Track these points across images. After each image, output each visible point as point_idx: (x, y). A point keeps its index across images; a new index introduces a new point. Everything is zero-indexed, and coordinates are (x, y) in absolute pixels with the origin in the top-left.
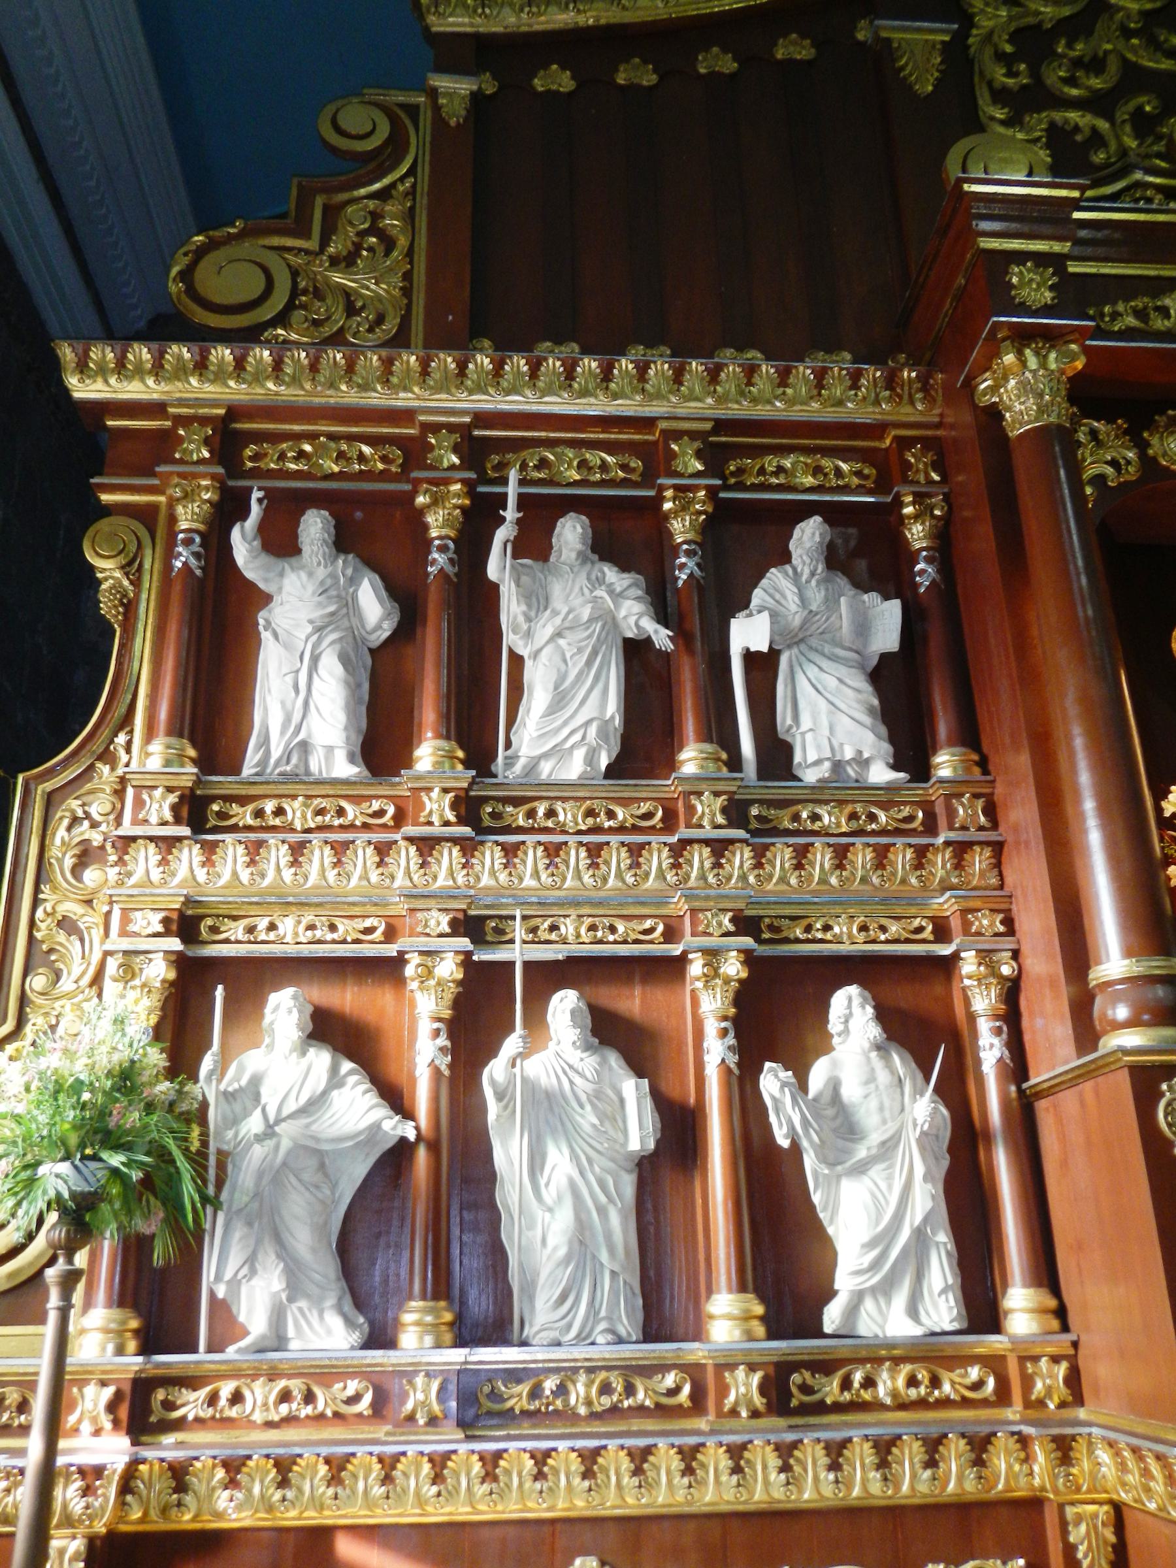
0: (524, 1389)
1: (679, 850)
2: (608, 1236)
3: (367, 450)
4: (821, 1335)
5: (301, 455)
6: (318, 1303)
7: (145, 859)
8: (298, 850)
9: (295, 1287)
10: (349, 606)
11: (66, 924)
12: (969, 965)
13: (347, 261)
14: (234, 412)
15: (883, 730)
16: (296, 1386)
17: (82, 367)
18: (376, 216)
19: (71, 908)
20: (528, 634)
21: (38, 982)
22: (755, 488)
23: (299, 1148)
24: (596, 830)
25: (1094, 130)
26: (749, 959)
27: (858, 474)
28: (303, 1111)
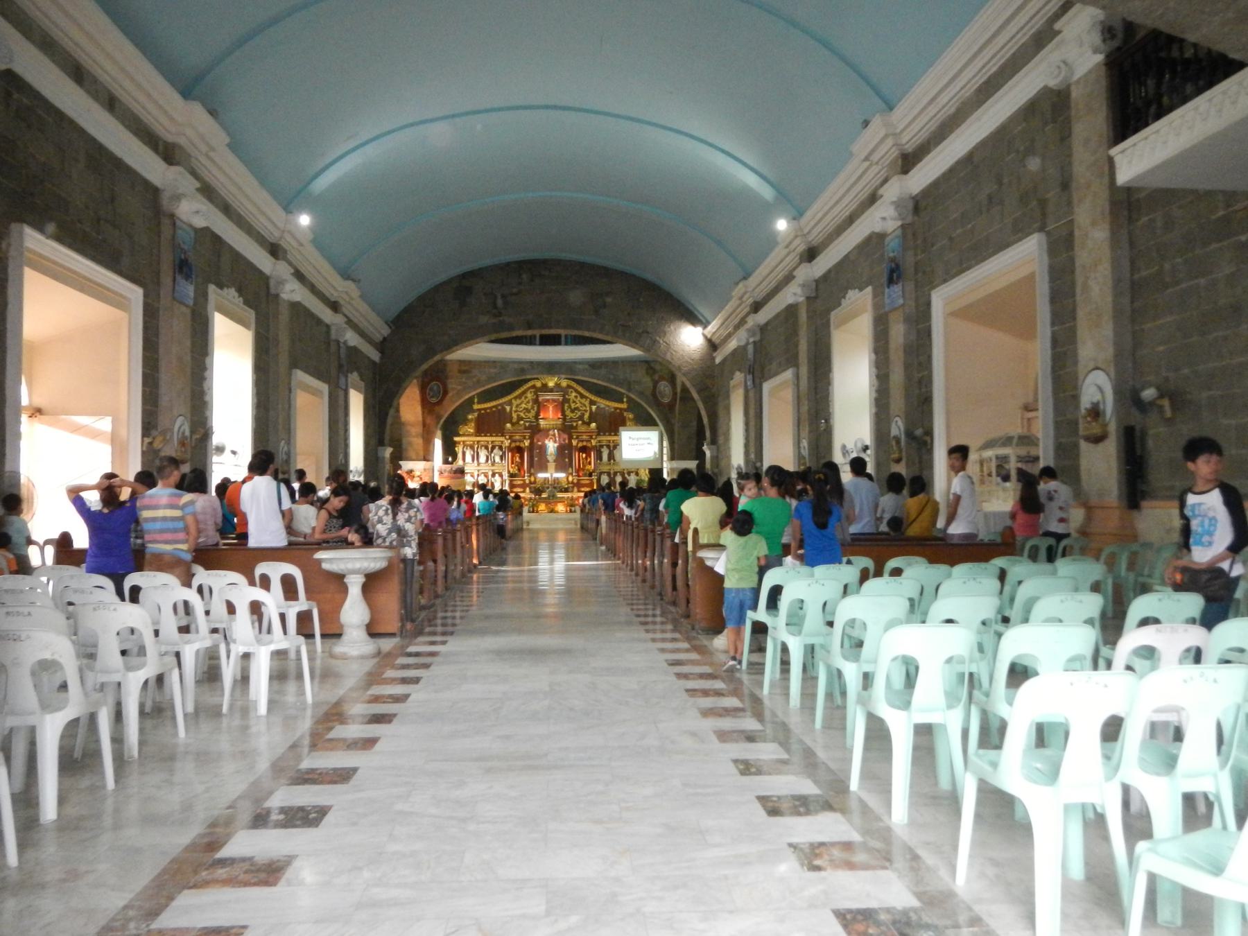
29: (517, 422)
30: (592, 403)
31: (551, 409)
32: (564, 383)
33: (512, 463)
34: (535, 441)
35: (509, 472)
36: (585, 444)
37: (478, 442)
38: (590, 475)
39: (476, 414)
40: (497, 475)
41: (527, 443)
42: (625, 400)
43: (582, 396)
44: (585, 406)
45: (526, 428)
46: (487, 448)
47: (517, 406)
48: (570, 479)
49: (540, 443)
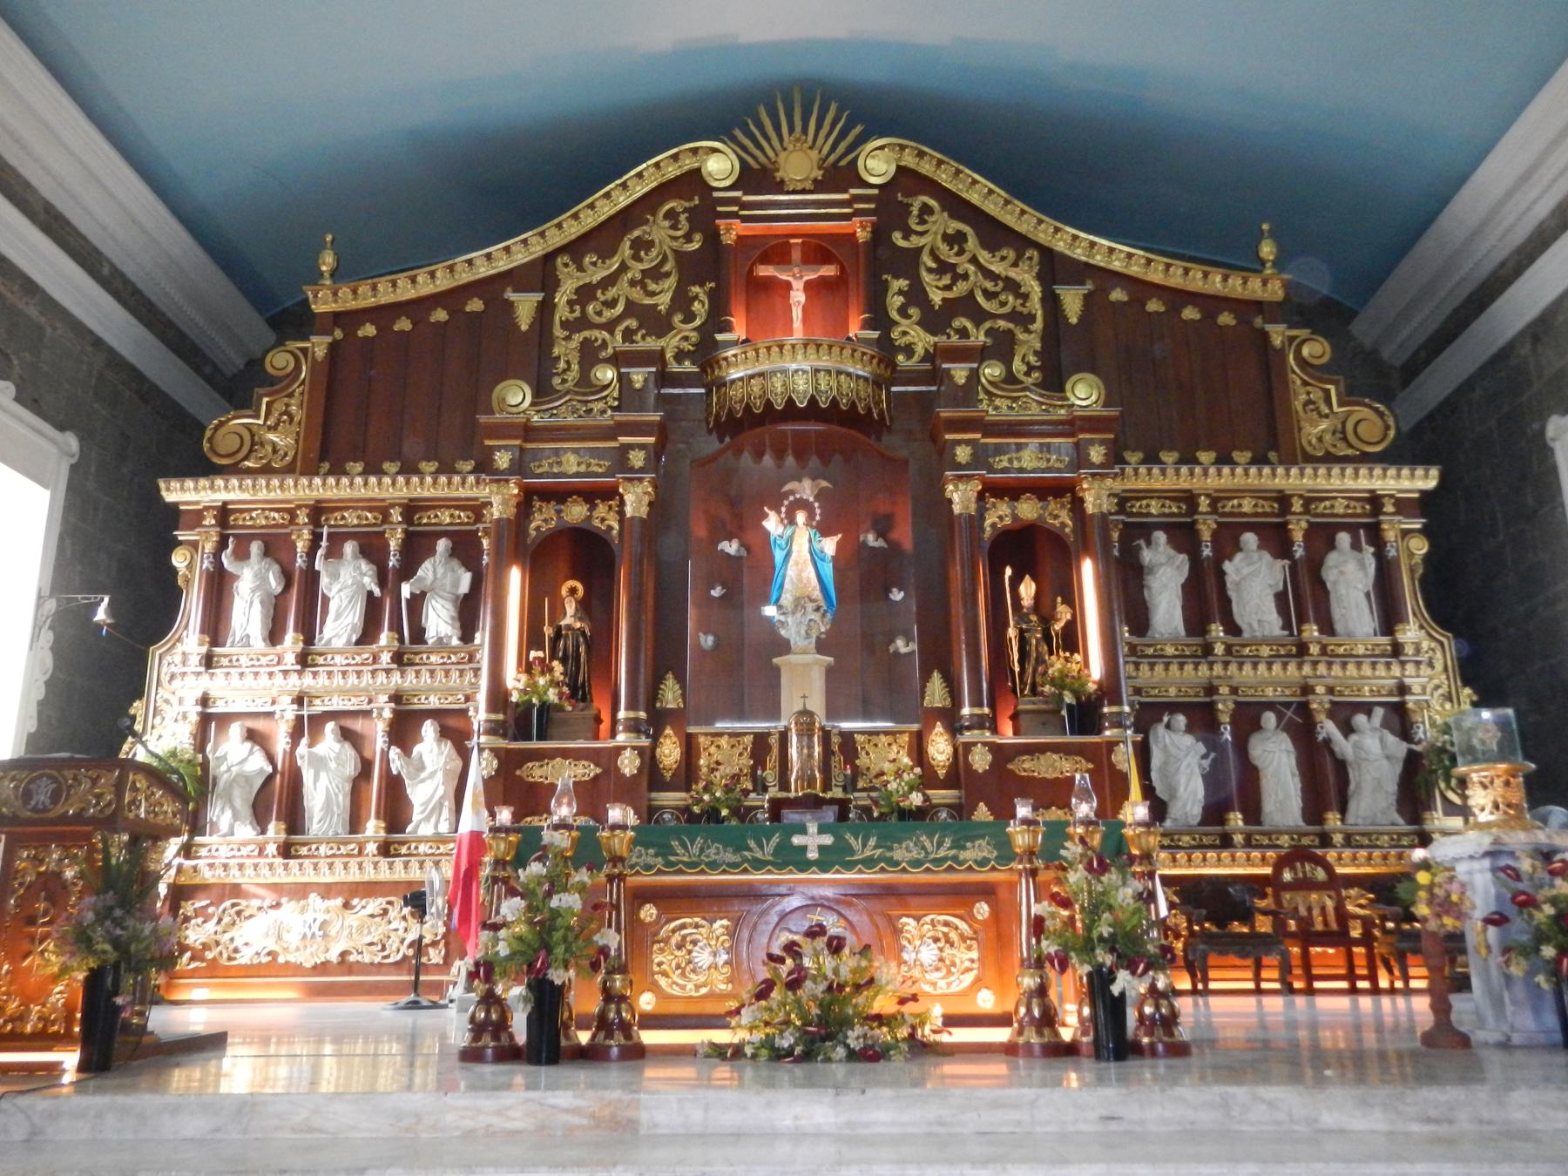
0: (305, 849)
1: (374, 672)
2: (338, 802)
3: (276, 515)
4: (404, 832)
5: (252, 518)
6: (243, 822)
7: (190, 679)
8: (242, 674)
9: (236, 817)
10: (265, 580)
11: (167, 701)
12: (471, 713)
13: (273, 429)
14: (225, 503)
15: (458, 625)
16: (235, 847)
17: (168, 489)
18: (287, 405)
19: (167, 696)
20: (330, 590)
21: (158, 720)
22: (425, 525)
23: (238, 775)
24: (348, 665)
25: (604, 341)
26: (394, 711)
27: (468, 517)
28: (240, 763)
29: (585, 381)
30: (1055, 268)
31: (798, 296)
32: (877, 165)
33: (532, 637)
34: (700, 530)
35: (498, 697)
36: (1028, 509)
37: (318, 511)
38: (1086, 716)
39: (319, 346)
40: (429, 729)
41: (636, 500)
42: (1267, 250)
43: (995, 234)
44: (1012, 286)
45: (628, 397)
46: (372, 549)
47: (585, 294)
48: (940, 749)
49: (731, 547)
